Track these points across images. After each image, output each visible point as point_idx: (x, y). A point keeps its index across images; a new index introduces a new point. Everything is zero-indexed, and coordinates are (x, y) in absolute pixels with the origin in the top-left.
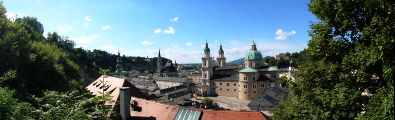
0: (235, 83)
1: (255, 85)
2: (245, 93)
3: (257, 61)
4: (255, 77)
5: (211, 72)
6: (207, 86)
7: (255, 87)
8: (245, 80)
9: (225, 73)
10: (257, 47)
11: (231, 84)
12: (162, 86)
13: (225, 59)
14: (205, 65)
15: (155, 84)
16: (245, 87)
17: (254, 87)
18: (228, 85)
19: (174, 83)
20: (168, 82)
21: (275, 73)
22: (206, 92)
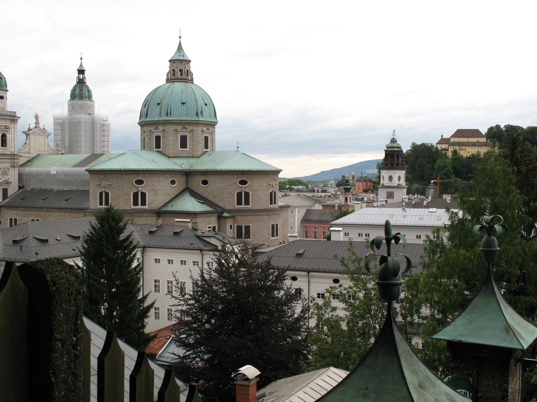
3: (179, 128)
10: (193, 68)
21: (243, 182)
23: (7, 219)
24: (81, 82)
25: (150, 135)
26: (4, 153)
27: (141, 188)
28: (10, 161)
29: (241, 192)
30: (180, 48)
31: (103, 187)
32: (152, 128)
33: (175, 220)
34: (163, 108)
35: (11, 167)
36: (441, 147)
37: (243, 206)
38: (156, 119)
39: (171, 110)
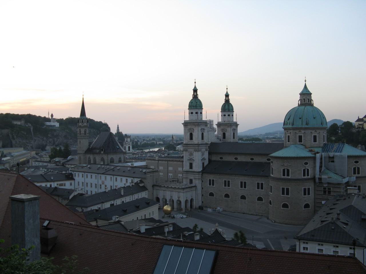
0: (260, 181)
1: (309, 189)
2: (285, 206)
3: (313, 131)
4: (308, 170)
5: (203, 155)
6: (194, 188)
7: (309, 194)
8: (284, 175)
9: (236, 159)
10: (313, 97)
11: (252, 182)
12: (89, 185)
13: (236, 125)
14: (191, 138)
15: (73, 182)
16: (283, 193)
17: (305, 194)
18: (243, 185)
19: (119, 178)
20: (103, 176)
21: (356, 162)
22: (192, 200)
23: (207, 180)
24: (227, 101)
25: (295, 135)
26: (203, 143)
27: (307, 167)
28: (205, 147)
29: (355, 168)
30: (305, 87)
31: (286, 166)
32: (297, 131)
33: (348, 188)
34: (303, 120)
35: (206, 151)
36: (359, 123)
37: (357, 175)
38: (300, 127)
39: (309, 122)
